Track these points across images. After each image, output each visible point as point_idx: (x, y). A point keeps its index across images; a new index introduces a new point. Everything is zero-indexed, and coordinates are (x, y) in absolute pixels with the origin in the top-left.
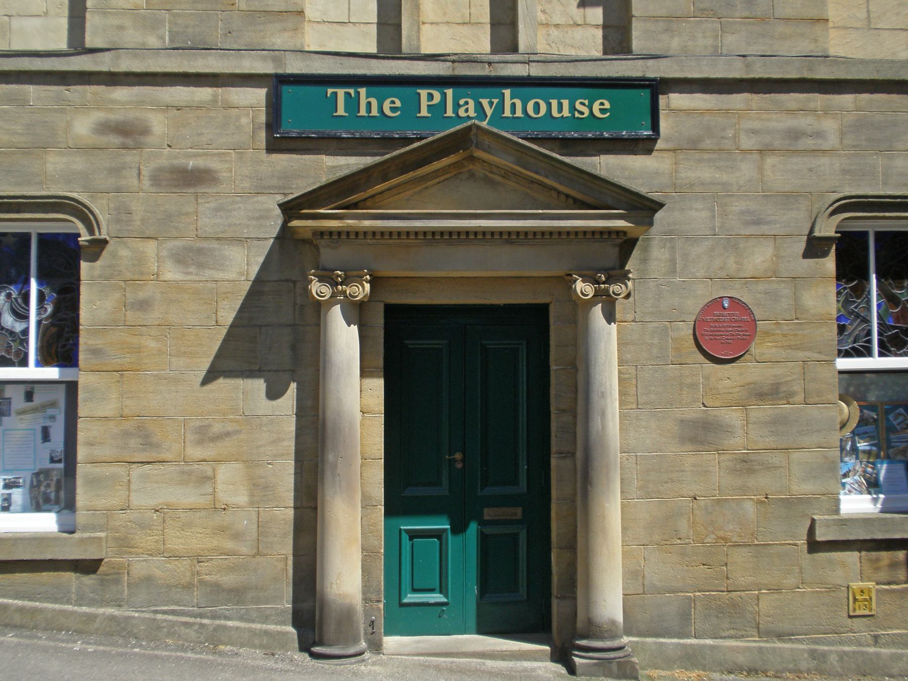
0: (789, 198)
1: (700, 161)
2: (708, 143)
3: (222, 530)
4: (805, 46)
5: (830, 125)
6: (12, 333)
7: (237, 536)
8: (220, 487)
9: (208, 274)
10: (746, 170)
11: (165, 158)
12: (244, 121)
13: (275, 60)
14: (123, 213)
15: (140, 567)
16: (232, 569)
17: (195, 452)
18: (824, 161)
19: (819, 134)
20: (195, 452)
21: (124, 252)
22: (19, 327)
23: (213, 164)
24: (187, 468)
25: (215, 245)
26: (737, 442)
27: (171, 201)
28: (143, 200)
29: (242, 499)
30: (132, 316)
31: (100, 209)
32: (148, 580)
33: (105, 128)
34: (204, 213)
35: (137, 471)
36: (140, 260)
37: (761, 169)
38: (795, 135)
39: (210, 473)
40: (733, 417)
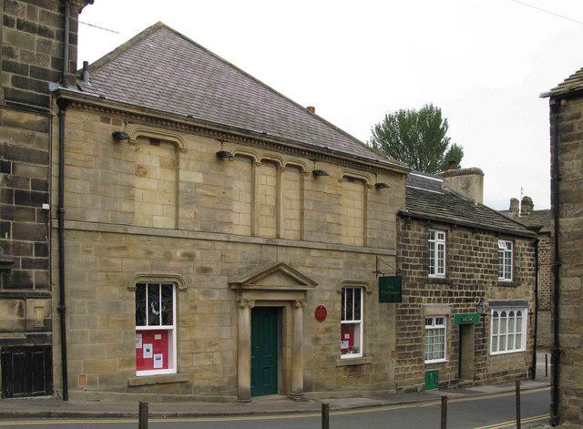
0: (333, 280)
2: (318, 265)
4: (336, 241)
5: (342, 262)
11: (199, 264)
13: (228, 237)
15: (196, 383)
16: (217, 382)
17: (208, 350)
18: (340, 272)
20: (208, 350)
23: (212, 266)
26: (322, 343)
27: (202, 277)
28: (195, 277)
30: (193, 311)
31: (184, 278)
32: (198, 387)
33: (185, 255)
36: (194, 293)
38: (335, 264)
40: (321, 336)
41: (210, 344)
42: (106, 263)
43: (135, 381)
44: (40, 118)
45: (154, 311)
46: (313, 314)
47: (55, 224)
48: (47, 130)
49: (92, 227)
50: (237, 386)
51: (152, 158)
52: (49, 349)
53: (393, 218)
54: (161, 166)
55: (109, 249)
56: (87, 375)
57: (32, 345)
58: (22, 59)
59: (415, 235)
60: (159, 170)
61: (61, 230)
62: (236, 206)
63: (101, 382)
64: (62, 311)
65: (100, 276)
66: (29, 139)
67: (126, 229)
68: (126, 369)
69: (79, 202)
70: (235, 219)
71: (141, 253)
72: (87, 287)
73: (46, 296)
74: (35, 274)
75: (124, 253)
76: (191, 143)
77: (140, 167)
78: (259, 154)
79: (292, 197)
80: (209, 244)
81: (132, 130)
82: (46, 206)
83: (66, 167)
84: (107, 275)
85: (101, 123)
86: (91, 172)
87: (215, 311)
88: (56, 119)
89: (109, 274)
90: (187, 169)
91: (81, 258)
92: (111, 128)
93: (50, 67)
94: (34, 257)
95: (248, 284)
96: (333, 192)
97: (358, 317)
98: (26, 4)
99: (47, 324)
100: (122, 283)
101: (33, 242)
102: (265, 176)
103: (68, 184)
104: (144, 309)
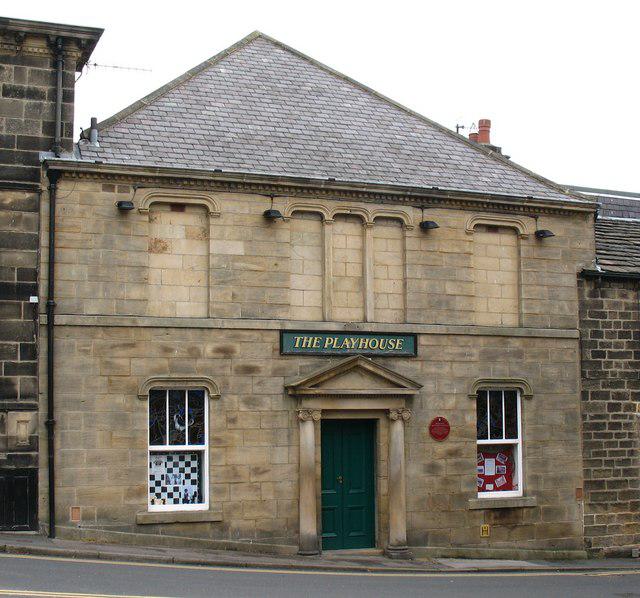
0: (462, 379)
2: (433, 358)
4: (465, 321)
6: (179, 431)
9: (257, 408)
10: (446, 369)
11: (241, 362)
14: (226, 385)
15: (234, 524)
17: (253, 479)
19: (471, 355)
20: (253, 479)
21: (226, 399)
22: (182, 429)
23: (258, 364)
26: (443, 473)
27: (244, 379)
30: (230, 426)
31: (218, 382)
33: (218, 350)
34: (251, 385)
35: (232, 486)
36: (232, 403)
37: (451, 368)
40: (442, 462)
41: (257, 471)
42: (108, 365)
43: (145, 517)
44: (28, 195)
45: (177, 426)
46: (426, 430)
47: (43, 319)
48: (37, 209)
49: (90, 321)
50: (298, 532)
51: (173, 228)
52: (34, 474)
53: (572, 281)
54: (187, 237)
55: (113, 347)
56: (81, 507)
57: (14, 467)
58: (8, 129)
59: (616, 305)
60: (184, 243)
61: (50, 326)
62: (297, 281)
63: (99, 517)
64: (50, 425)
65: (101, 381)
66: (17, 221)
67: (134, 321)
68: (134, 502)
69: (74, 293)
70: (295, 298)
71: (155, 352)
72: (83, 396)
73: (33, 408)
74: (19, 381)
75: (132, 351)
76: (222, 202)
77: (158, 241)
78: (329, 207)
79: (388, 263)
80: (256, 335)
81: (141, 198)
82: (33, 299)
83: (57, 250)
84: (110, 381)
85: (102, 193)
86: (90, 253)
87: (264, 425)
88: (45, 196)
89: (113, 378)
90: (221, 238)
91: (75, 360)
92: (115, 196)
93: (40, 134)
94: (19, 361)
96: (457, 250)
97: (512, 434)
98: (13, 67)
99: (33, 443)
100: (132, 391)
101: (19, 343)
102: (343, 237)
103: (61, 271)
104: (164, 422)
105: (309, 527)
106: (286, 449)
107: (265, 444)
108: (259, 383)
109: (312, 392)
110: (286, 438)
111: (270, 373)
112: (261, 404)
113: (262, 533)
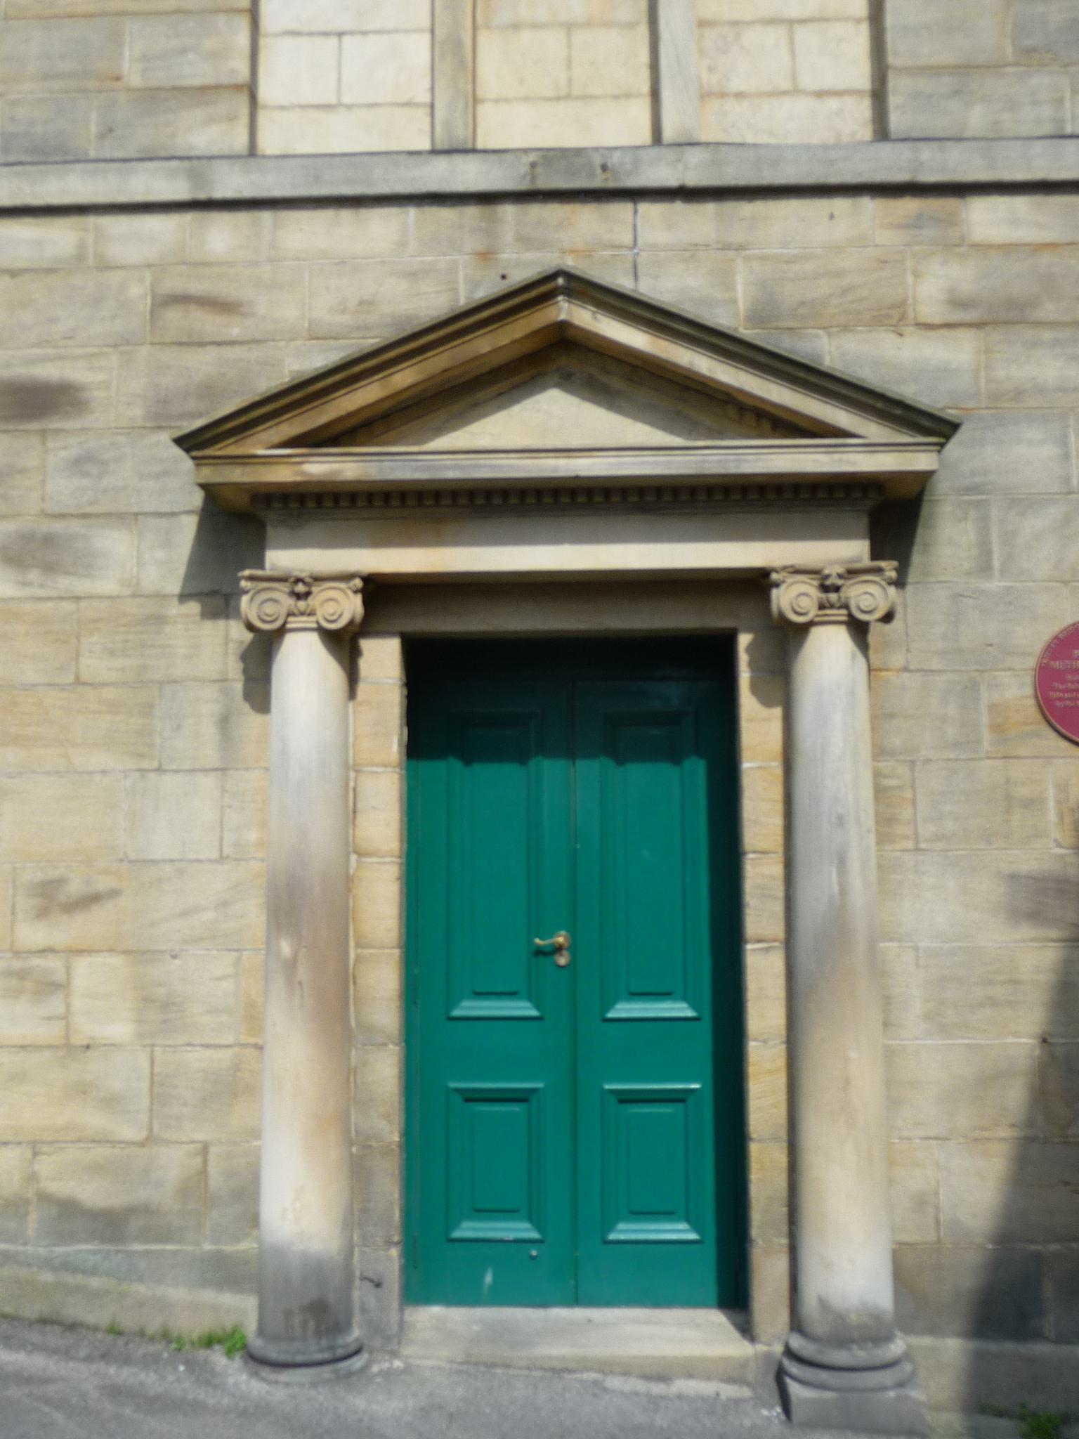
1: (1035, 344)
2: (1049, 310)
3: (82, 1090)
7: (111, 1102)
8: (78, 1003)
9: (64, 583)
12: (135, 291)
13: (196, 177)
16: (98, 1169)
17: (33, 934)
24: (17, 964)
25: (75, 526)
29: (120, 1030)
39: (60, 976)
46: (1017, 690)
50: (254, 1220)
80: (60, 237)
87: (94, 665)
95: (259, 444)
105: (302, 1204)
106: (208, 782)
107: (98, 759)
108: (79, 464)
109: (283, 475)
110: (210, 732)
111: (138, 412)
112: (84, 564)
113: (69, 1216)
